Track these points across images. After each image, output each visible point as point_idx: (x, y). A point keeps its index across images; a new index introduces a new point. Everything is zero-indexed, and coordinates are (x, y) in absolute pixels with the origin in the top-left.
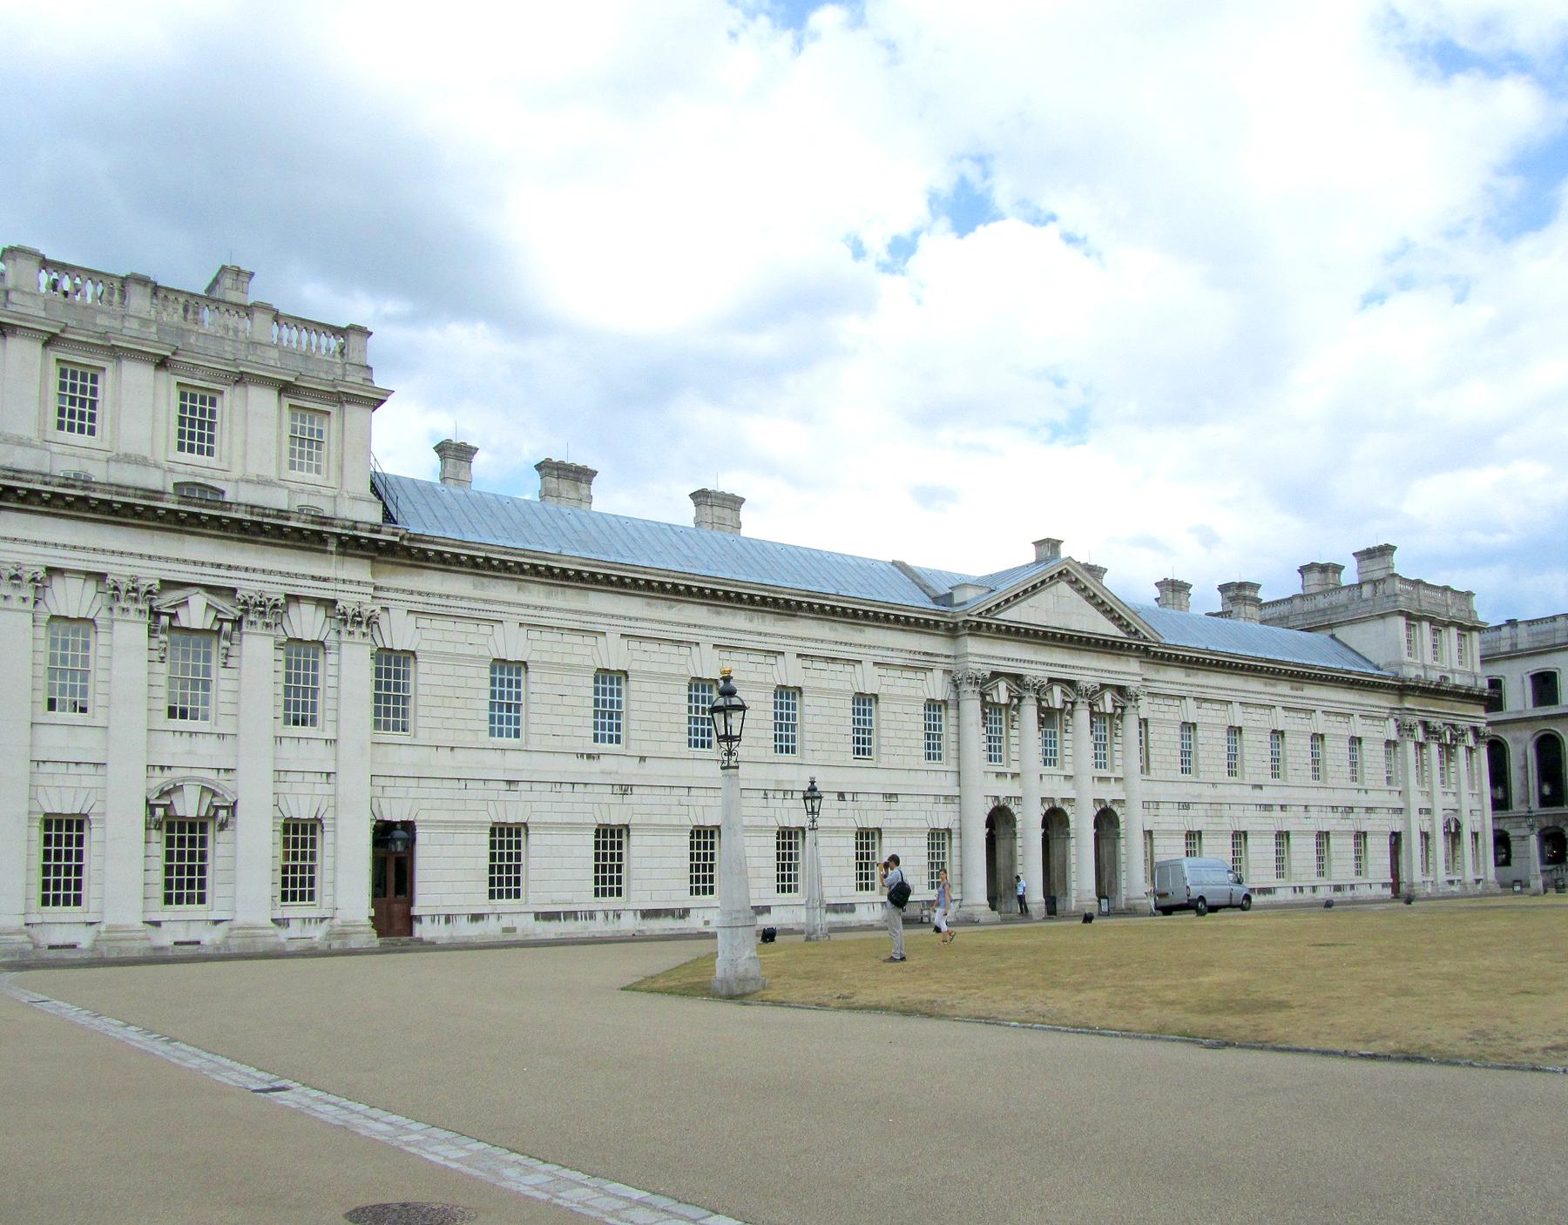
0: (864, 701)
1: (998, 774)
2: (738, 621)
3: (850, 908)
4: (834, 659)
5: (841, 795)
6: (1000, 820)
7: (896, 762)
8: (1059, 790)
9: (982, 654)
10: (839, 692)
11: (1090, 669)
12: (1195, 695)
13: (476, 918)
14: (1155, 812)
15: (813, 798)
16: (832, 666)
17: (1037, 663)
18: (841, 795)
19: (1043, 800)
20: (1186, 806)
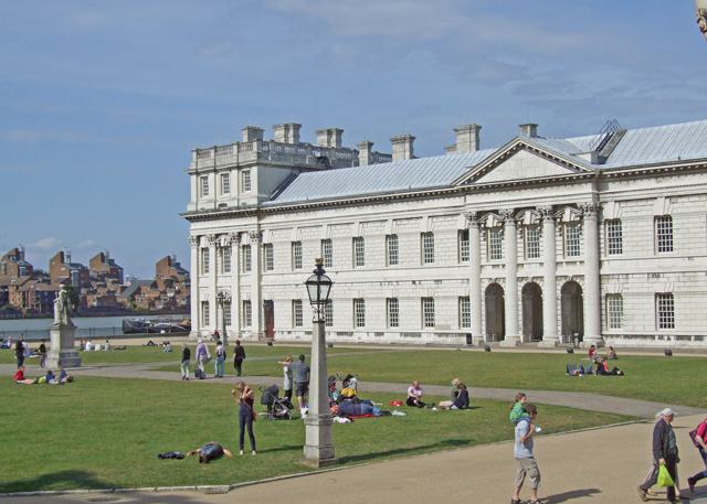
0: (427, 236)
1: (494, 266)
2: (368, 210)
3: (419, 335)
4: (411, 219)
5: (414, 282)
6: (495, 292)
7: (442, 264)
8: (530, 271)
9: (476, 202)
10: (413, 234)
11: (546, 198)
12: (666, 195)
13: (289, 332)
14: (625, 281)
15: (319, 283)
16: (411, 222)
17: (506, 201)
18: (414, 282)
19: (519, 279)
20: (656, 275)
